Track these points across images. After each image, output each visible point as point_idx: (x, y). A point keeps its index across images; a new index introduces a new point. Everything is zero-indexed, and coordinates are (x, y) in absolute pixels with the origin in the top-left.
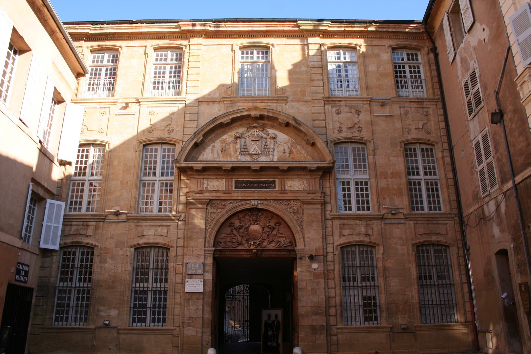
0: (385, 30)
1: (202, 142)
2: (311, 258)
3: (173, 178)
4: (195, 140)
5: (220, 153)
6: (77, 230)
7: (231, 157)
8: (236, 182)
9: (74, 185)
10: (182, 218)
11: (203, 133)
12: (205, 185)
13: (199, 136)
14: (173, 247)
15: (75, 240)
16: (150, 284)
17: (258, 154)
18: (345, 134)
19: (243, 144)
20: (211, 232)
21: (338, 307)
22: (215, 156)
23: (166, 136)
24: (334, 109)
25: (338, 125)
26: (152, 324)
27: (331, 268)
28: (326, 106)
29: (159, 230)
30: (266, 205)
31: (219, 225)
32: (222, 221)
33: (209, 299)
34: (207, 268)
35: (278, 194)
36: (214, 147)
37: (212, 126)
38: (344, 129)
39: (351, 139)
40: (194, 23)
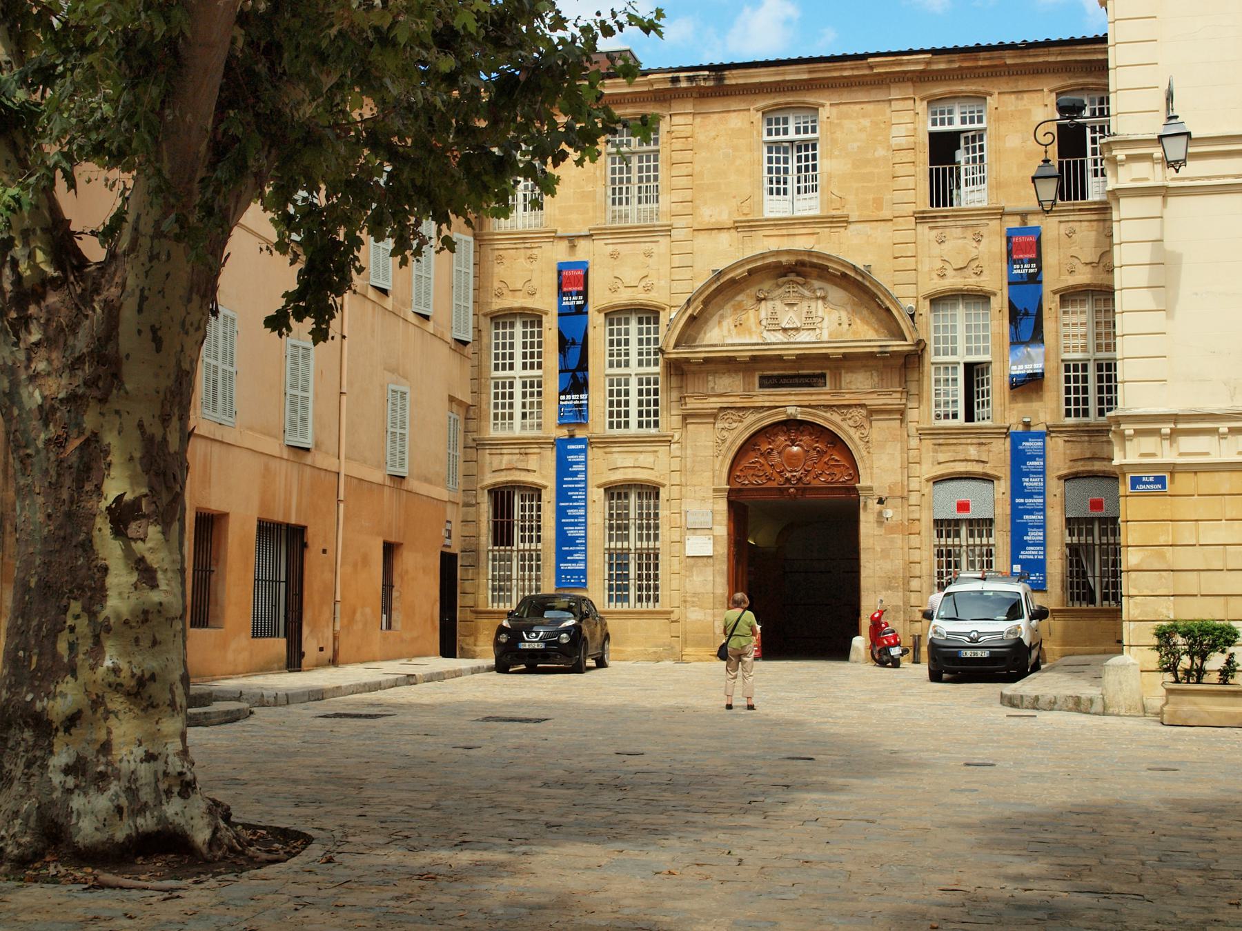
0: (1041, 59)
1: (701, 312)
2: (881, 501)
3: (657, 369)
4: (690, 311)
5: (732, 327)
6: (510, 462)
7: (750, 333)
8: (761, 378)
9: (496, 387)
10: (676, 438)
11: (701, 298)
12: (711, 384)
13: (696, 303)
14: (664, 486)
15: (510, 479)
16: (633, 543)
17: (796, 329)
18: (953, 281)
19: (770, 311)
20: (723, 462)
21: (925, 578)
22: (725, 333)
23: (641, 297)
24: (934, 232)
25: (940, 264)
26: (638, 605)
27: (916, 516)
28: (919, 226)
29: (641, 457)
30: (810, 414)
31: (735, 449)
32: (739, 442)
33: (723, 566)
34: (718, 518)
35: (828, 397)
36: (722, 317)
37: (715, 286)
38: (950, 272)
39: (961, 290)
40: (676, 75)
